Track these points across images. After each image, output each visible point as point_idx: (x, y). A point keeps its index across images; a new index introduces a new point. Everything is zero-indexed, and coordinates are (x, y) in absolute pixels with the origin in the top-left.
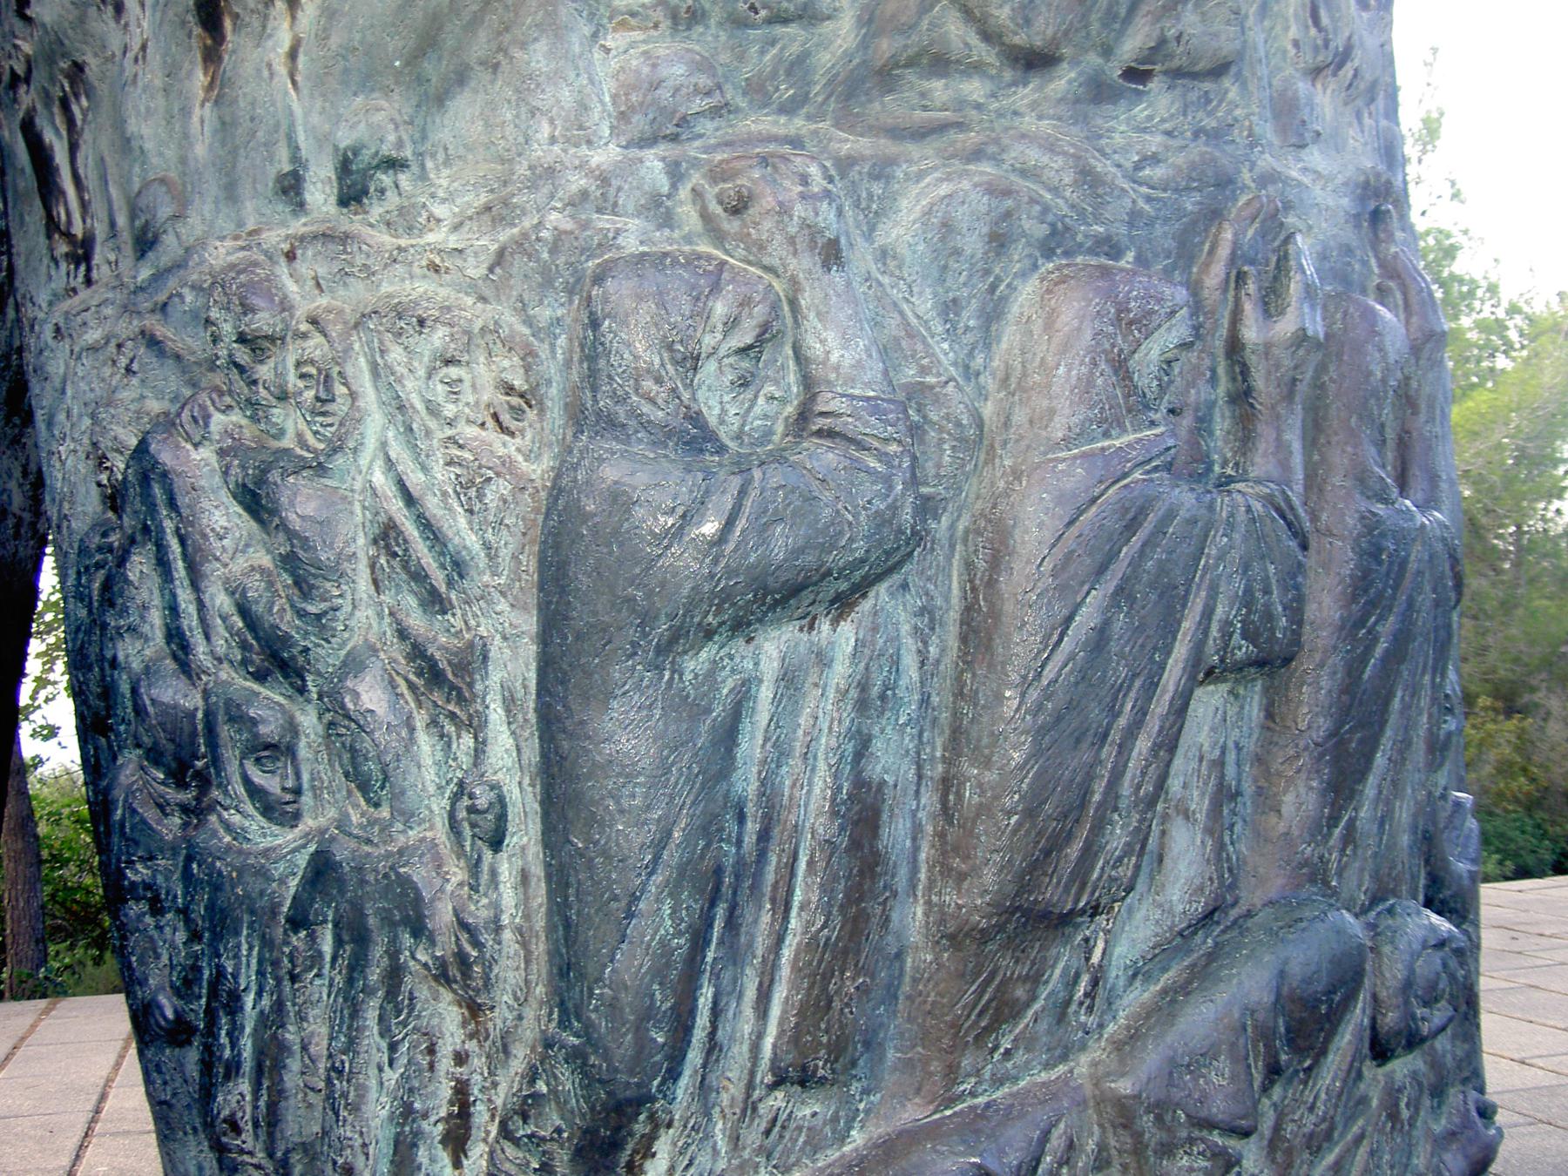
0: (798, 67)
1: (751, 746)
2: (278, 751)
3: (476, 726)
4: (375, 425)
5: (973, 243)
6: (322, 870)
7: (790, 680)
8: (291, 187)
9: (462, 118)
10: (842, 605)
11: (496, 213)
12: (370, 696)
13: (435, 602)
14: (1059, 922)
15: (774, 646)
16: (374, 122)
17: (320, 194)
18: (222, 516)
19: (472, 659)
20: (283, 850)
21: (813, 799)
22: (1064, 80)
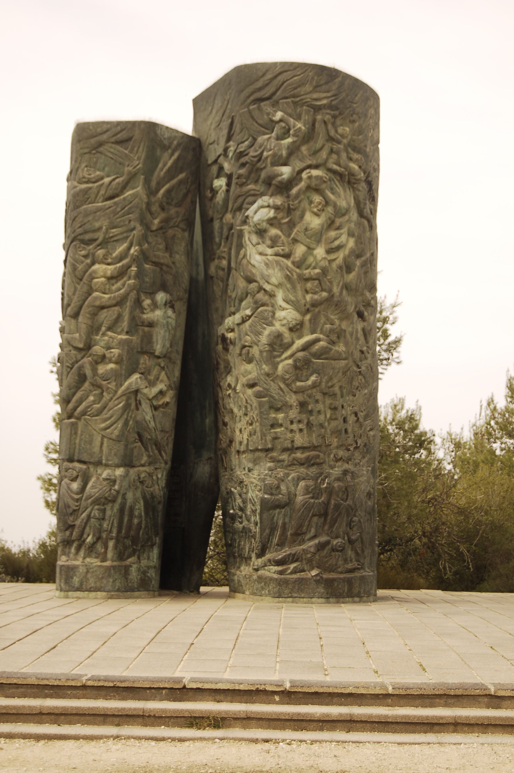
0: (282, 465)
1: (275, 518)
2: (241, 517)
3: (256, 516)
4: (250, 491)
5: (296, 479)
6: (244, 528)
7: (279, 513)
8: (244, 469)
9: (257, 467)
10: (283, 508)
11: (259, 475)
12: (249, 513)
13: (253, 505)
14: (299, 535)
15: (277, 511)
16: (250, 465)
17: (246, 469)
18: (238, 496)
19: (256, 510)
20: (241, 526)
21: (280, 522)
22: (306, 466)
